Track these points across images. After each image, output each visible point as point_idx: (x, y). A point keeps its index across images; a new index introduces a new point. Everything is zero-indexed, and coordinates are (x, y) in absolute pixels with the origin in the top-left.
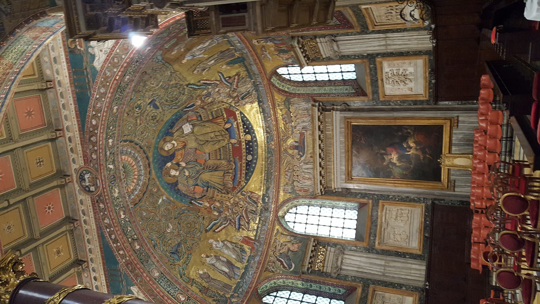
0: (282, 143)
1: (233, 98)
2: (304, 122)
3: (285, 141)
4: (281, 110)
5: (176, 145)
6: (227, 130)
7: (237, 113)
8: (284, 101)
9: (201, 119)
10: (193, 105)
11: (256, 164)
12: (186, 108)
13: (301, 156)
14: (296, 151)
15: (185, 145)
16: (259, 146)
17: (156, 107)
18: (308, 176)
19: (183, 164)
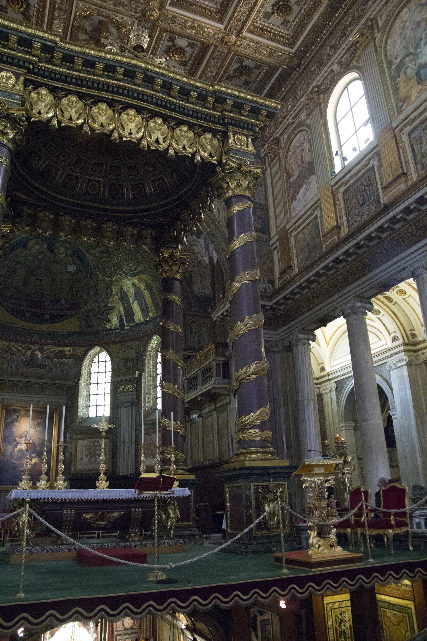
0: (38, 347)
1: (88, 312)
2: (57, 370)
3: (39, 350)
4: (69, 351)
5: (60, 256)
6: (59, 300)
7: (73, 312)
8: (77, 355)
9: (75, 281)
10: (91, 279)
11: (21, 319)
12: (91, 273)
13: (23, 363)
14: (29, 359)
15: (56, 262)
16: (36, 325)
17: (102, 252)
18: (4, 367)
19: (40, 257)
